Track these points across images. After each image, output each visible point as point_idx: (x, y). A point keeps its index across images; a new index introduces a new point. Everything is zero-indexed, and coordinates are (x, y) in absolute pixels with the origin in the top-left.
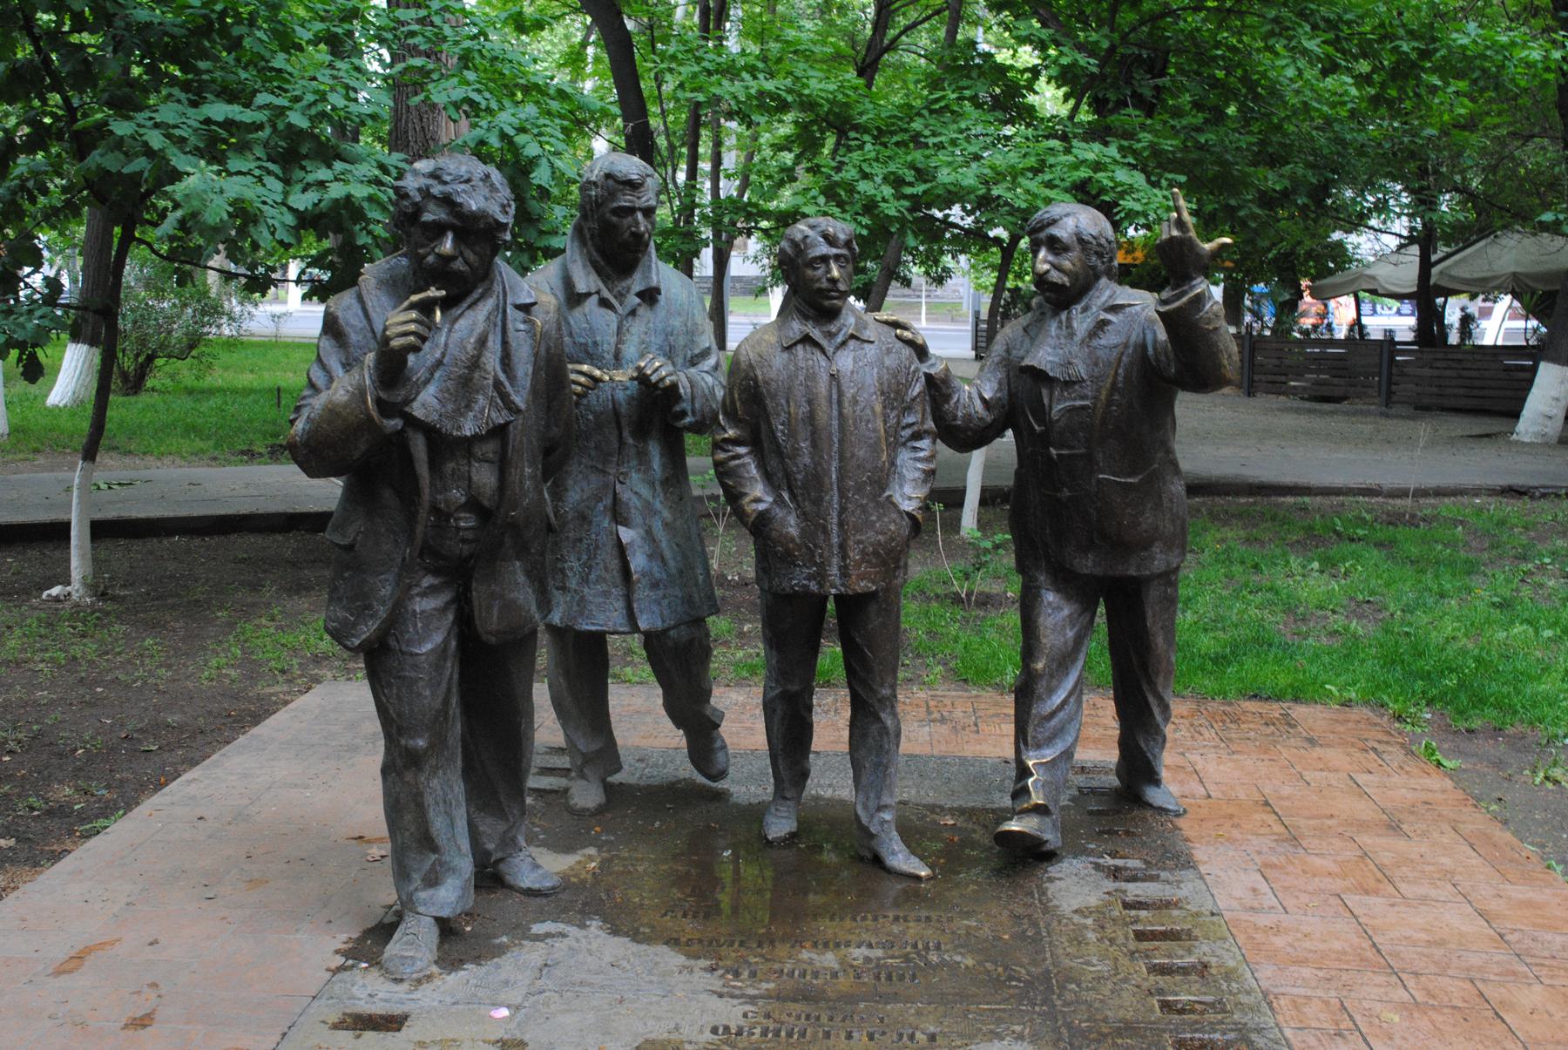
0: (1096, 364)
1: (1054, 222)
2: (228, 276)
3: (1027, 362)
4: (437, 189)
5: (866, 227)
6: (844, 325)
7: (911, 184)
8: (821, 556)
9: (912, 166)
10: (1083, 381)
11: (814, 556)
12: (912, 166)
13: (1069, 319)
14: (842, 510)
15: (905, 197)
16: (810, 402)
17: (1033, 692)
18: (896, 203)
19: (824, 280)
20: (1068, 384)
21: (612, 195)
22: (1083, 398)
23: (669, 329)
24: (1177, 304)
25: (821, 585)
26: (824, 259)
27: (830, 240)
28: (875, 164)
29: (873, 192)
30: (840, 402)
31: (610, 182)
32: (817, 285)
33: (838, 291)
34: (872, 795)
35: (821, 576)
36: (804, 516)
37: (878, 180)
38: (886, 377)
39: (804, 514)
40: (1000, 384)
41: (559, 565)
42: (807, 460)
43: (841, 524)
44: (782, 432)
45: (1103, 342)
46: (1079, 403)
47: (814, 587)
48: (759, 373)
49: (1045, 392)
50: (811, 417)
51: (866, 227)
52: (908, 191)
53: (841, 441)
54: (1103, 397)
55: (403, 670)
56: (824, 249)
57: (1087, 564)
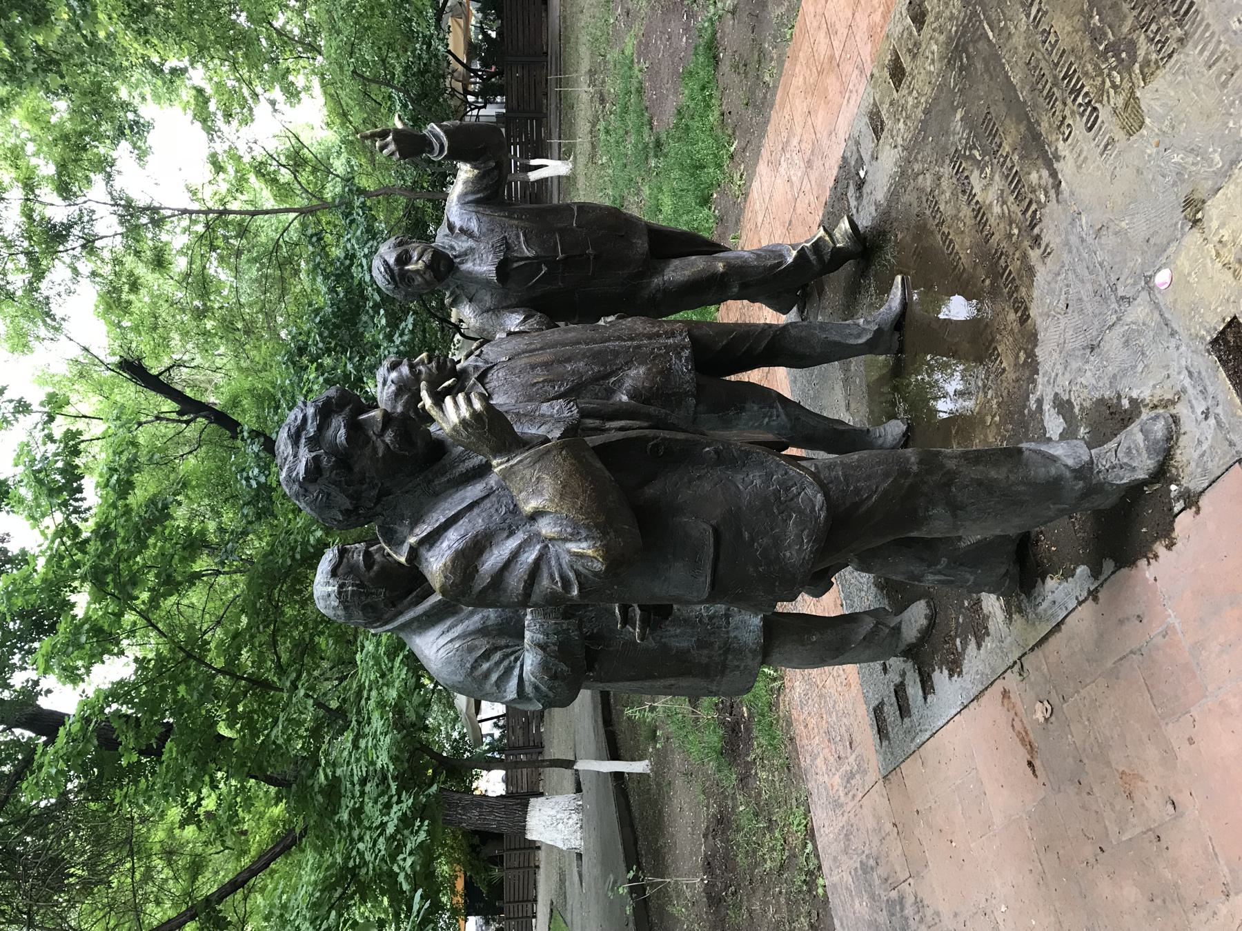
0: (493, 230)
1: (386, 262)
2: (372, 247)
3: (493, 276)
4: (311, 429)
5: (422, 821)
8: (659, 349)
10: (505, 238)
11: (661, 354)
13: (459, 256)
14: (619, 338)
16: (533, 367)
17: (741, 267)
19: (430, 366)
20: (508, 248)
21: (352, 569)
22: (518, 237)
24: (442, 134)
25: (682, 349)
26: (412, 367)
27: (394, 367)
30: (531, 351)
31: (340, 571)
32: (434, 370)
34: (848, 331)
35: (678, 349)
36: (628, 364)
37: (385, 819)
39: (626, 363)
40: (513, 313)
41: (706, 621)
42: (582, 364)
43: (632, 339)
44: (560, 387)
45: (476, 230)
46: (522, 238)
47: (686, 353)
49: (515, 265)
50: (546, 365)
51: (422, 821)
53: (564, 345)
54: (516, 222)
55: (837, 478)
56: (405, 370)
57: (641, 244)
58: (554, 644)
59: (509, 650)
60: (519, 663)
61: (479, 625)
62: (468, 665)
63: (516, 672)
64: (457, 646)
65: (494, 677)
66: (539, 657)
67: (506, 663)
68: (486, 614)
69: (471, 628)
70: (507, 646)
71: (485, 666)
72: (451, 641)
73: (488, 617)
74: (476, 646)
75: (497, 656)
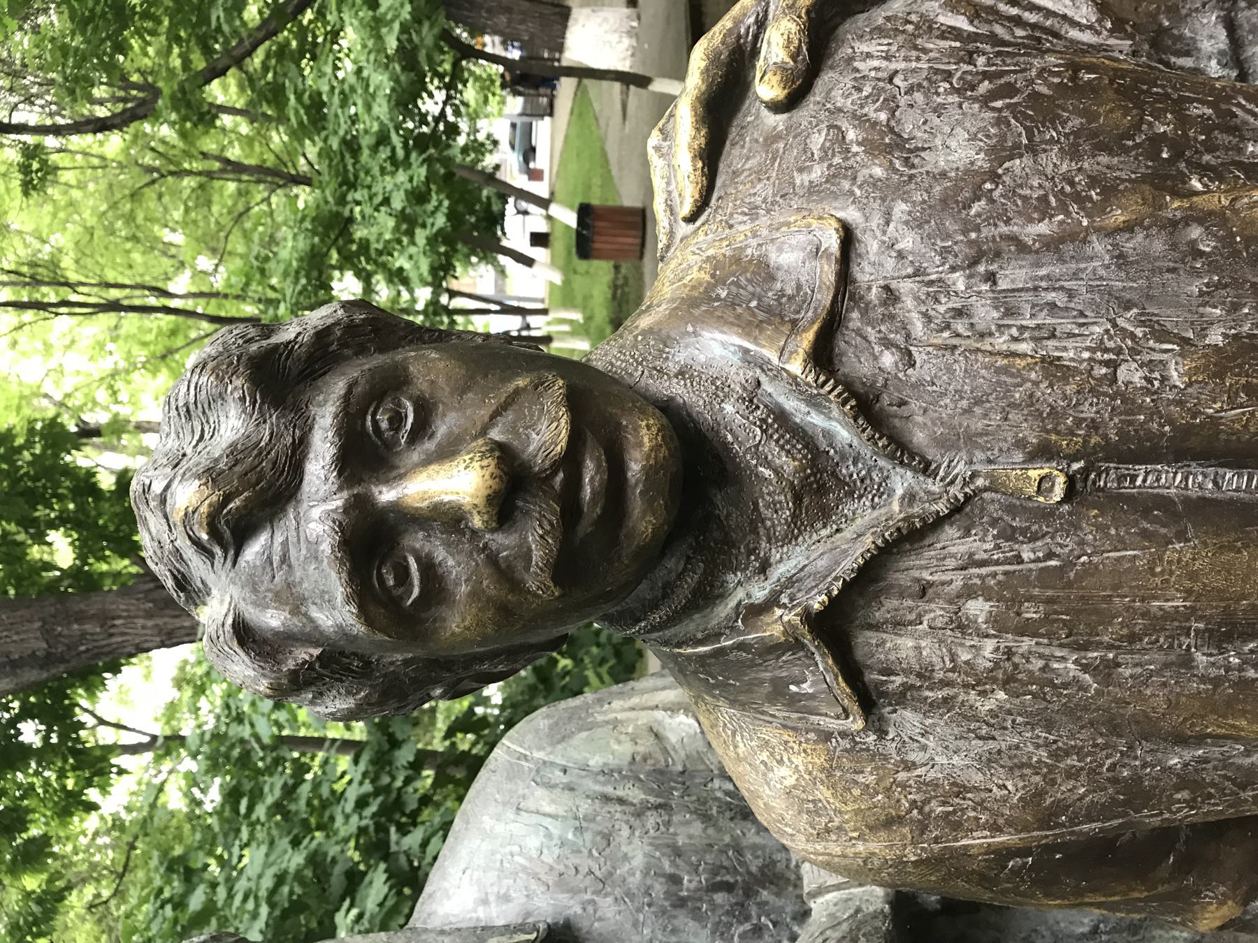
6: (751, 397)
7: (393, 150)
9: (375, 149)
12: (375, 149)
15: (407, 156)
18: (414, 166)
23: (659, 889)
28: (374, 190)
29: (402, 193)
32: (536, 579)
33: (571, 460)
38: (1051, 159)
48: (977, 840)
52: (400, 153)
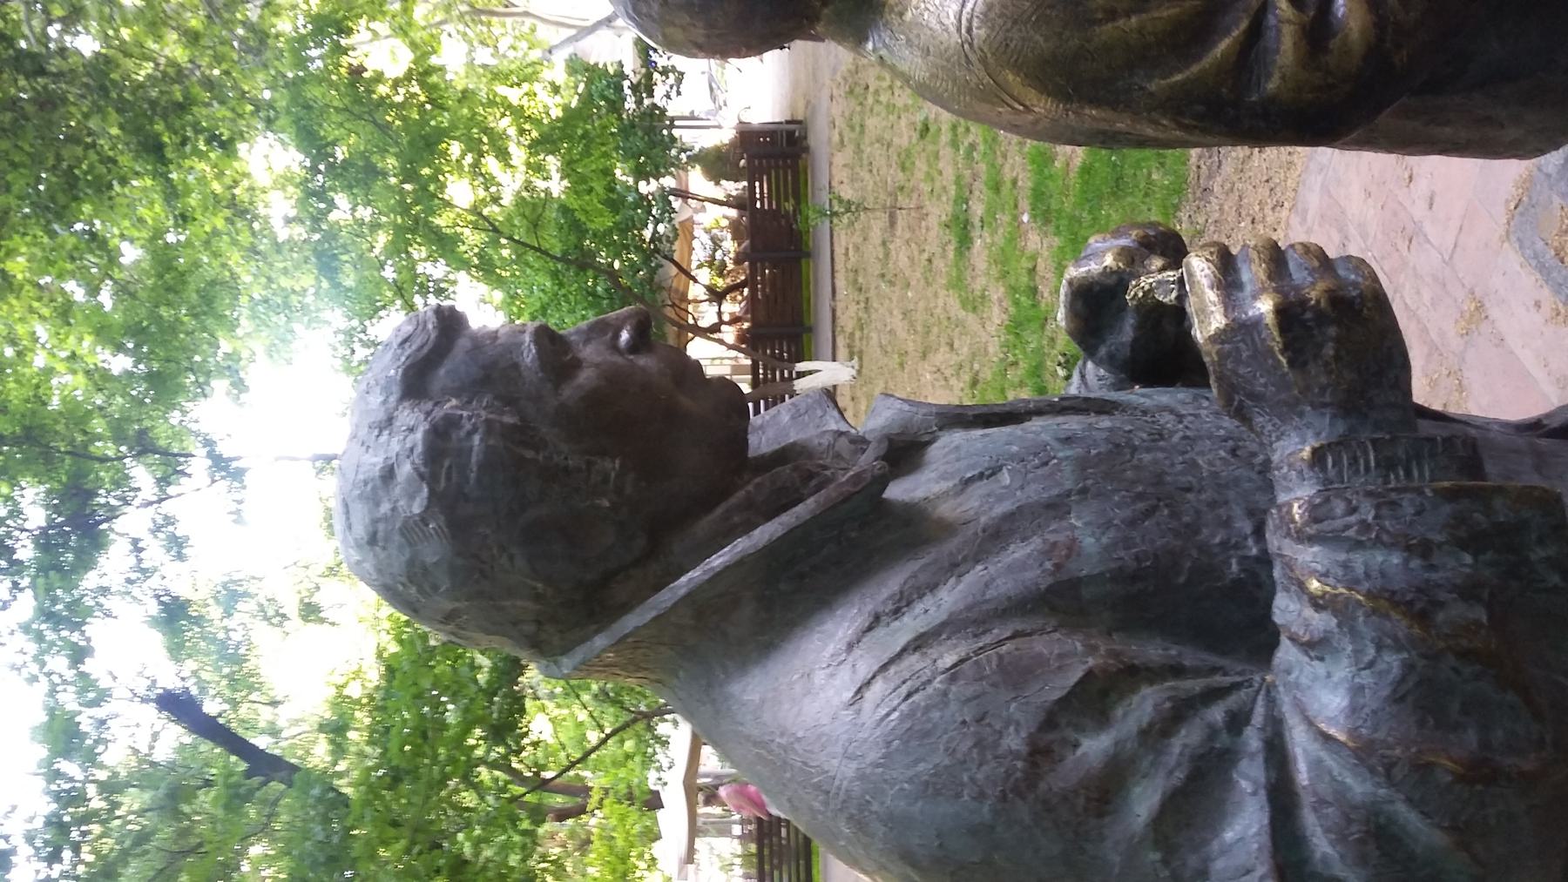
31: (442, 376)
58: (1469, 592)
59: (1195, 685)
60: (1253, 739)
61: (1036, 577)
62: (1014, 741)
63: (1249, 777)
64: (949, 660)
65: (1144, 801)
66: (1393, 662)
67: (1187, 738)
68: (1061, 538)
69: (1005, 587)
70: (1177, 671)
71: (1095, 747)
72: (919, 644)
73: (1072, 547)
74: (1040, 661)
75: (1144, 705)
